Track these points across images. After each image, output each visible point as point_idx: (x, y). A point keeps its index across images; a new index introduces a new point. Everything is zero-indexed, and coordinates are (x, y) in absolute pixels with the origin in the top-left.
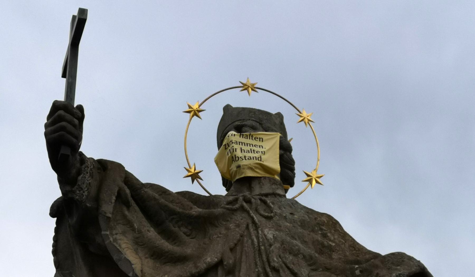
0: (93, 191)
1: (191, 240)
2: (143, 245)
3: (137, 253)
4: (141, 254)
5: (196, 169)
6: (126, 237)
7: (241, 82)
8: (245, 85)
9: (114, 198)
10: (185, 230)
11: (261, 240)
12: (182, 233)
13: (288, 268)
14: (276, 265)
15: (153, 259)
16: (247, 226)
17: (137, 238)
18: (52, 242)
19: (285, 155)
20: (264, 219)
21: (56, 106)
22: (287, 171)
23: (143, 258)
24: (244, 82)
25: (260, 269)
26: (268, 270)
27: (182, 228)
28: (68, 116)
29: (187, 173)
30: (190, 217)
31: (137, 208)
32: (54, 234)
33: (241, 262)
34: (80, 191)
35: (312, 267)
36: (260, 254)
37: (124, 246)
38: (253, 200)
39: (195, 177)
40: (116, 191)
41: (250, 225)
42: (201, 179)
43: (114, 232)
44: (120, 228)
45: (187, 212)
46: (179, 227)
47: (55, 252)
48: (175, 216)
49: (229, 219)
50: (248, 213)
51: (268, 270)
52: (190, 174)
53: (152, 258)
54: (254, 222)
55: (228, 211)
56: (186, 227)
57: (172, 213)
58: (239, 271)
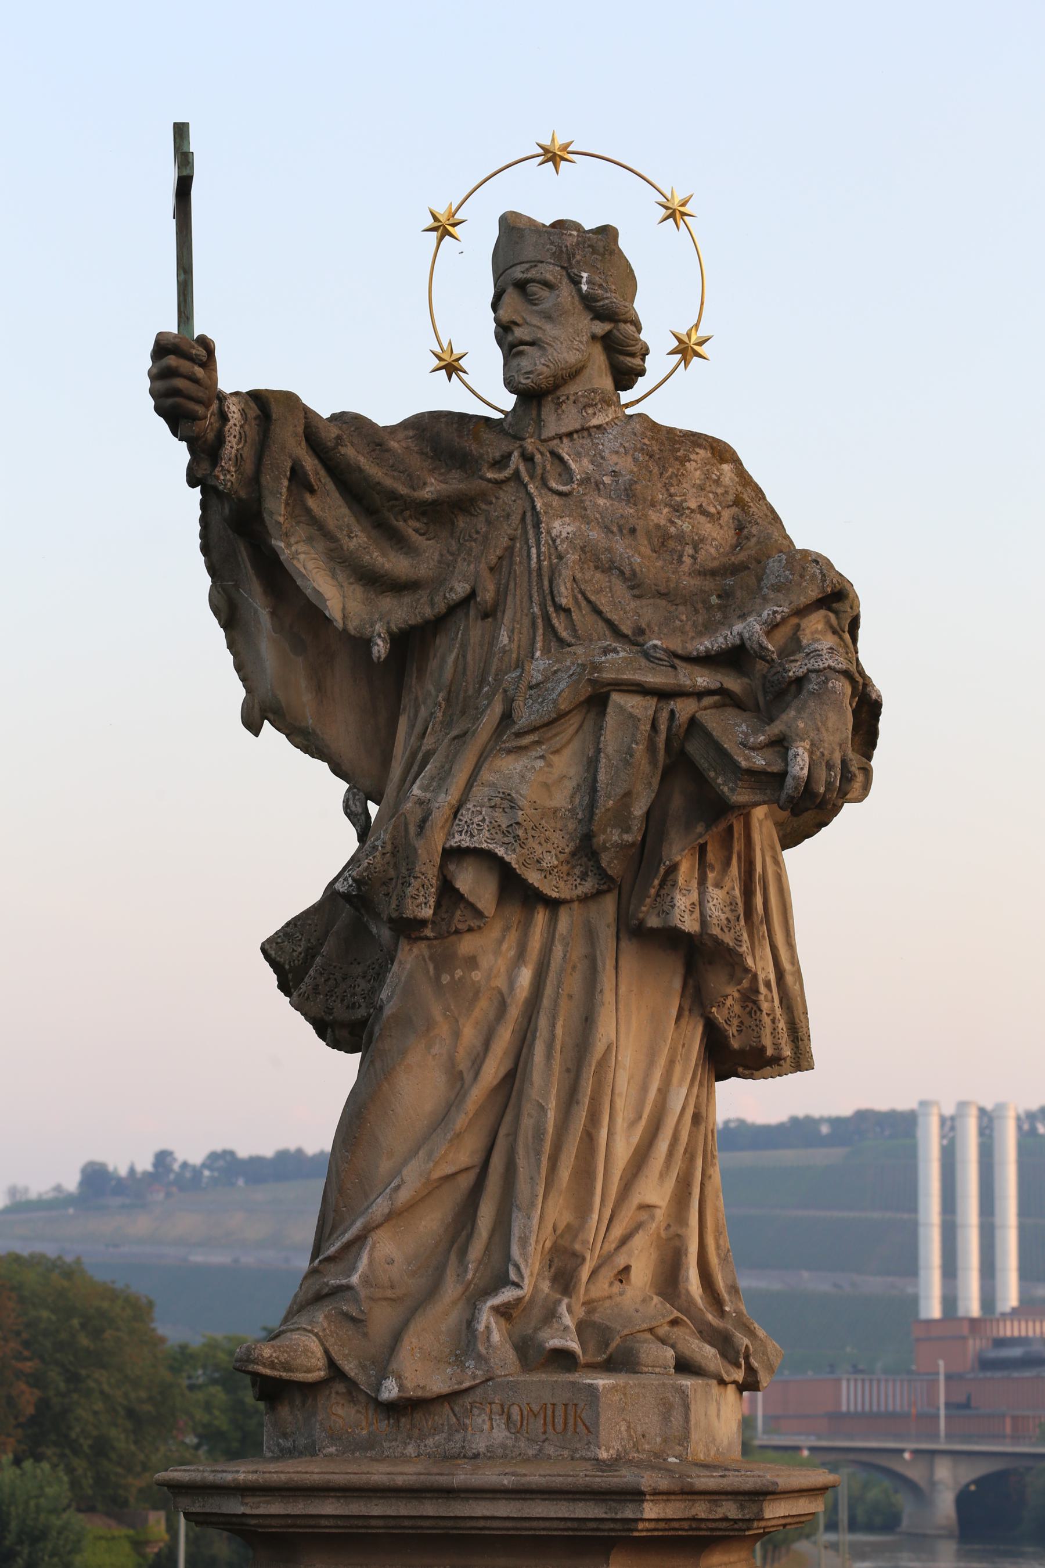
0: (249, 467)
1: (428, 542)
2: (343, 563)
3: (334, 576)
4: (341, 577)
5: (454, 352)
6: (313, 547)
7: (450, 343)
8: (546, 150)
9: (285, 483)
10: (417, 525)
11: (543, 549)
12: (410, 531)
13: (589, 601)
14: (564, 601)
15: (363, 586)
16: (524, 514)
17: (331, 550)
18: (198, 528)
19: (615, 331)
20: (557, 498)
21: (163, 348)
22: (622, 358)
23: (345, 584)
24: (546, 142)
25: (536, 609)
26: (551, 609)
27: (411, 523)
28: (184, 365)
29: (436, 362)
30: (424, 503)
31: (331, 486)
32: (200, 512)
33: (506, 595)
34: (225, 475)
35: (636, 592)
36: (540, 575)
37: (310, 565)
38: (538, 457)
39: (451, 368)
40: (288, 469)
41: (529, 514)
42: (465, 372)
43: (293, 540)
44: (301, 531)
45: (416, 494)
46: (405, 521)
47: (205, 549)
48: (397, 503)
49: (494, 500)
50: (525, 486)
51: (551, 609)
52: (443, 363)
53: (361, 583)
54: (534, 508)
55: (490, 485)
56: (418, 520)
57: (393, 496)
58: (504, 612)
